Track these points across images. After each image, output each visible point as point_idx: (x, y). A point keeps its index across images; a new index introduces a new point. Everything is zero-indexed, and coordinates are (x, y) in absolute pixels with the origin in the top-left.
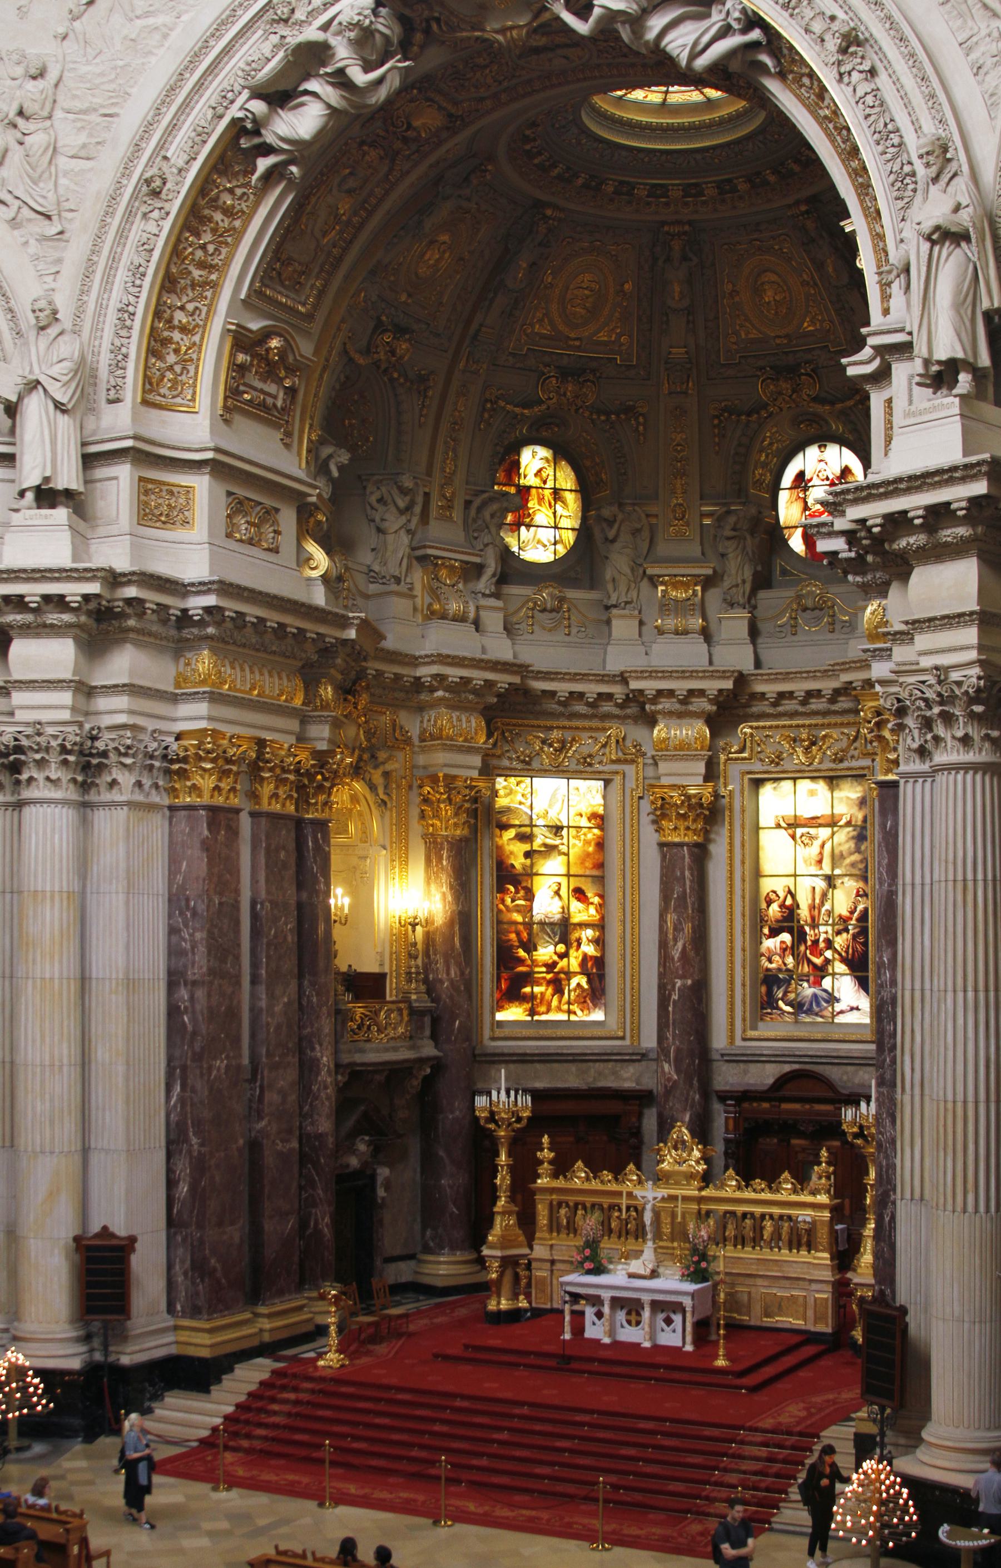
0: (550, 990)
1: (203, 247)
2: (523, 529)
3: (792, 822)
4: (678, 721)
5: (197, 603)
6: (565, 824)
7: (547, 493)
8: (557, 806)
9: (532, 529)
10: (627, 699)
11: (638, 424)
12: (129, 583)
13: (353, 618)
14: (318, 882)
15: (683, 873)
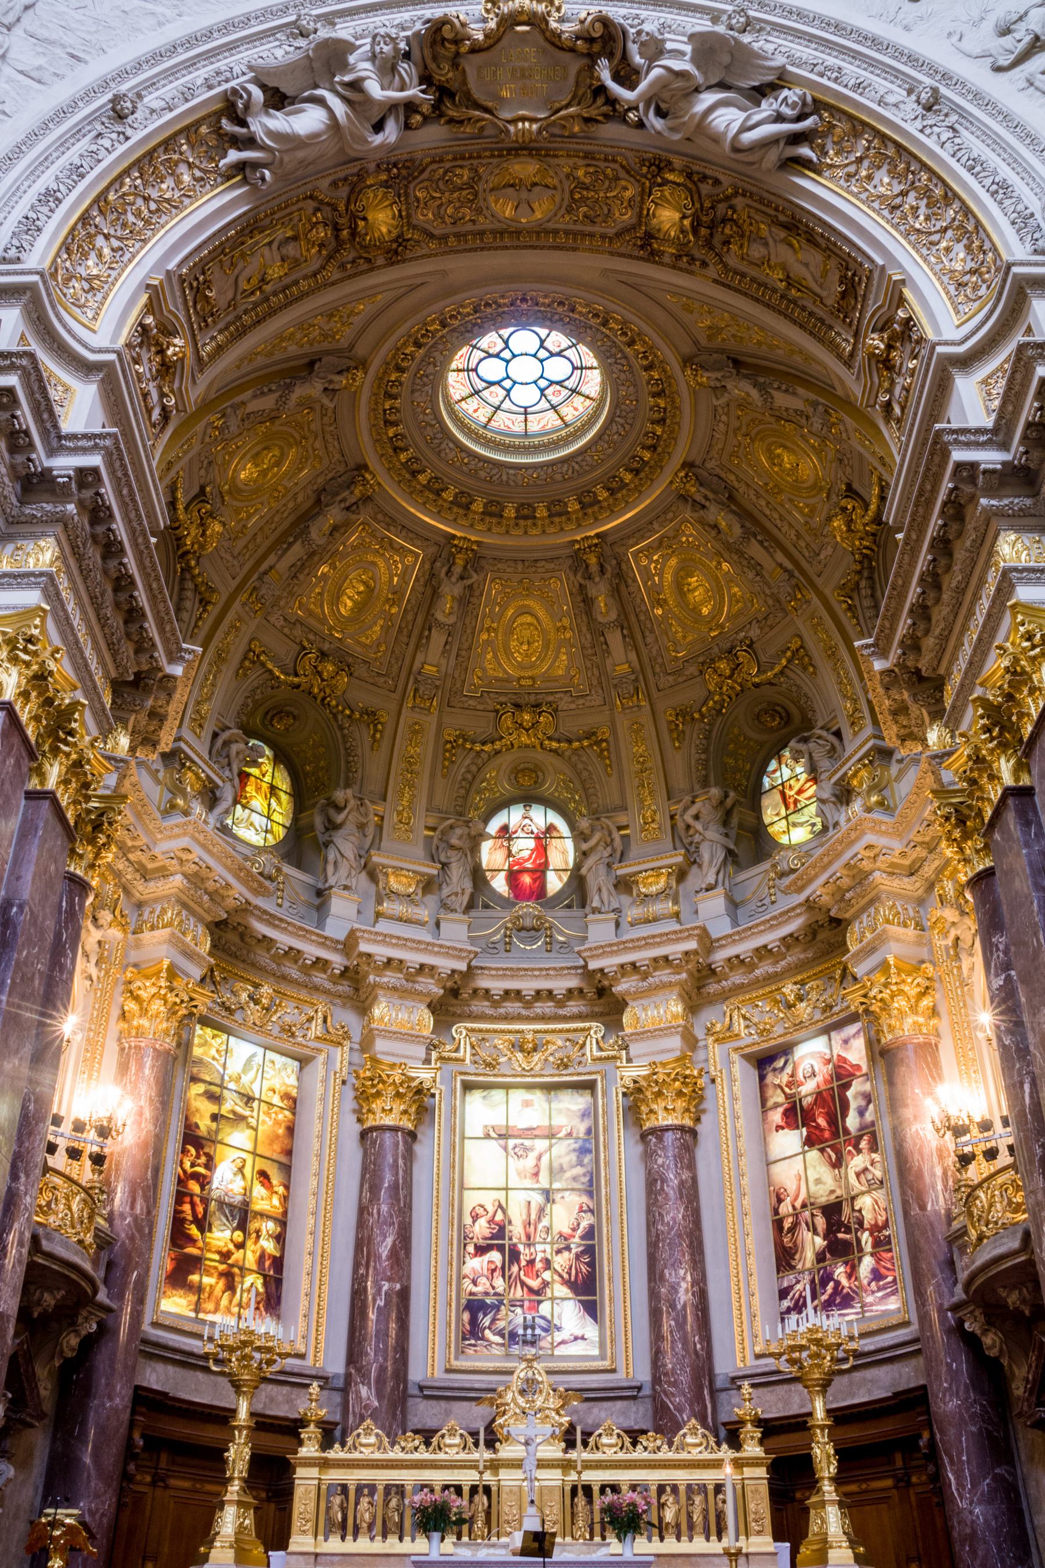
0: (221, 1285)
1: (147, 199)
2: (239, 807)
3: (503, 1132)
4: (399, 1001)
5: (64, 464)
6: (257, 1096)
7: (265, 786)
8: (251, 1074)
9: (247, 811)
10: (345, 972)
11: (376, 731)
12: (12, 368)
13: (186, 651)
14: (66, 956)
15: (396, 1161)
